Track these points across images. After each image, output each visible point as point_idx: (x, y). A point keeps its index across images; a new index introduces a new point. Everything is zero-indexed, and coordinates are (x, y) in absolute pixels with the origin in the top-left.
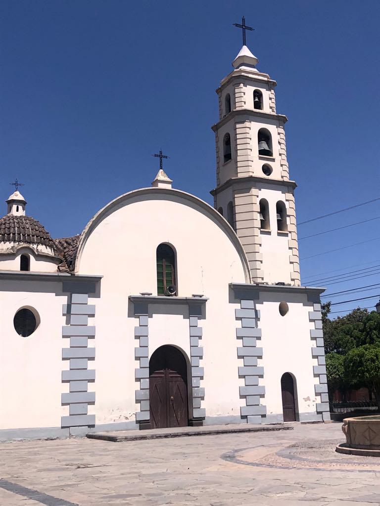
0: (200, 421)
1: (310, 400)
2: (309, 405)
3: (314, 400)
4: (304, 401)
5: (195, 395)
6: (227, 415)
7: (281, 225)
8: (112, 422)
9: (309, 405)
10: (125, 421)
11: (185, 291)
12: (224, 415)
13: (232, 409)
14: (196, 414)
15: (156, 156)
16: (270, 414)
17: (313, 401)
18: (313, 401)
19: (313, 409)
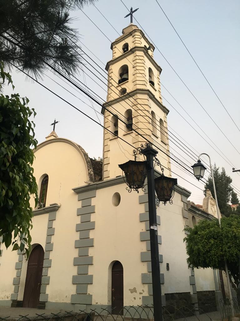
0: (42, 306)
1: (136, 292)
2: (135, 298)
3: (142, 292)
4: (130, 291)
5: (43, 282)
6: (62, 301)
7: (129, 127)
8: (1, 300)
9: (135, 298)
10: (7, 299)
11: (49, 203)
12: (59, 302)
13: (66, 296)
14: (41, 299)
15: (52, 124)
16: (95, 304)
17: (140, 293)
18: (140, 293)
19: (138, 302)
